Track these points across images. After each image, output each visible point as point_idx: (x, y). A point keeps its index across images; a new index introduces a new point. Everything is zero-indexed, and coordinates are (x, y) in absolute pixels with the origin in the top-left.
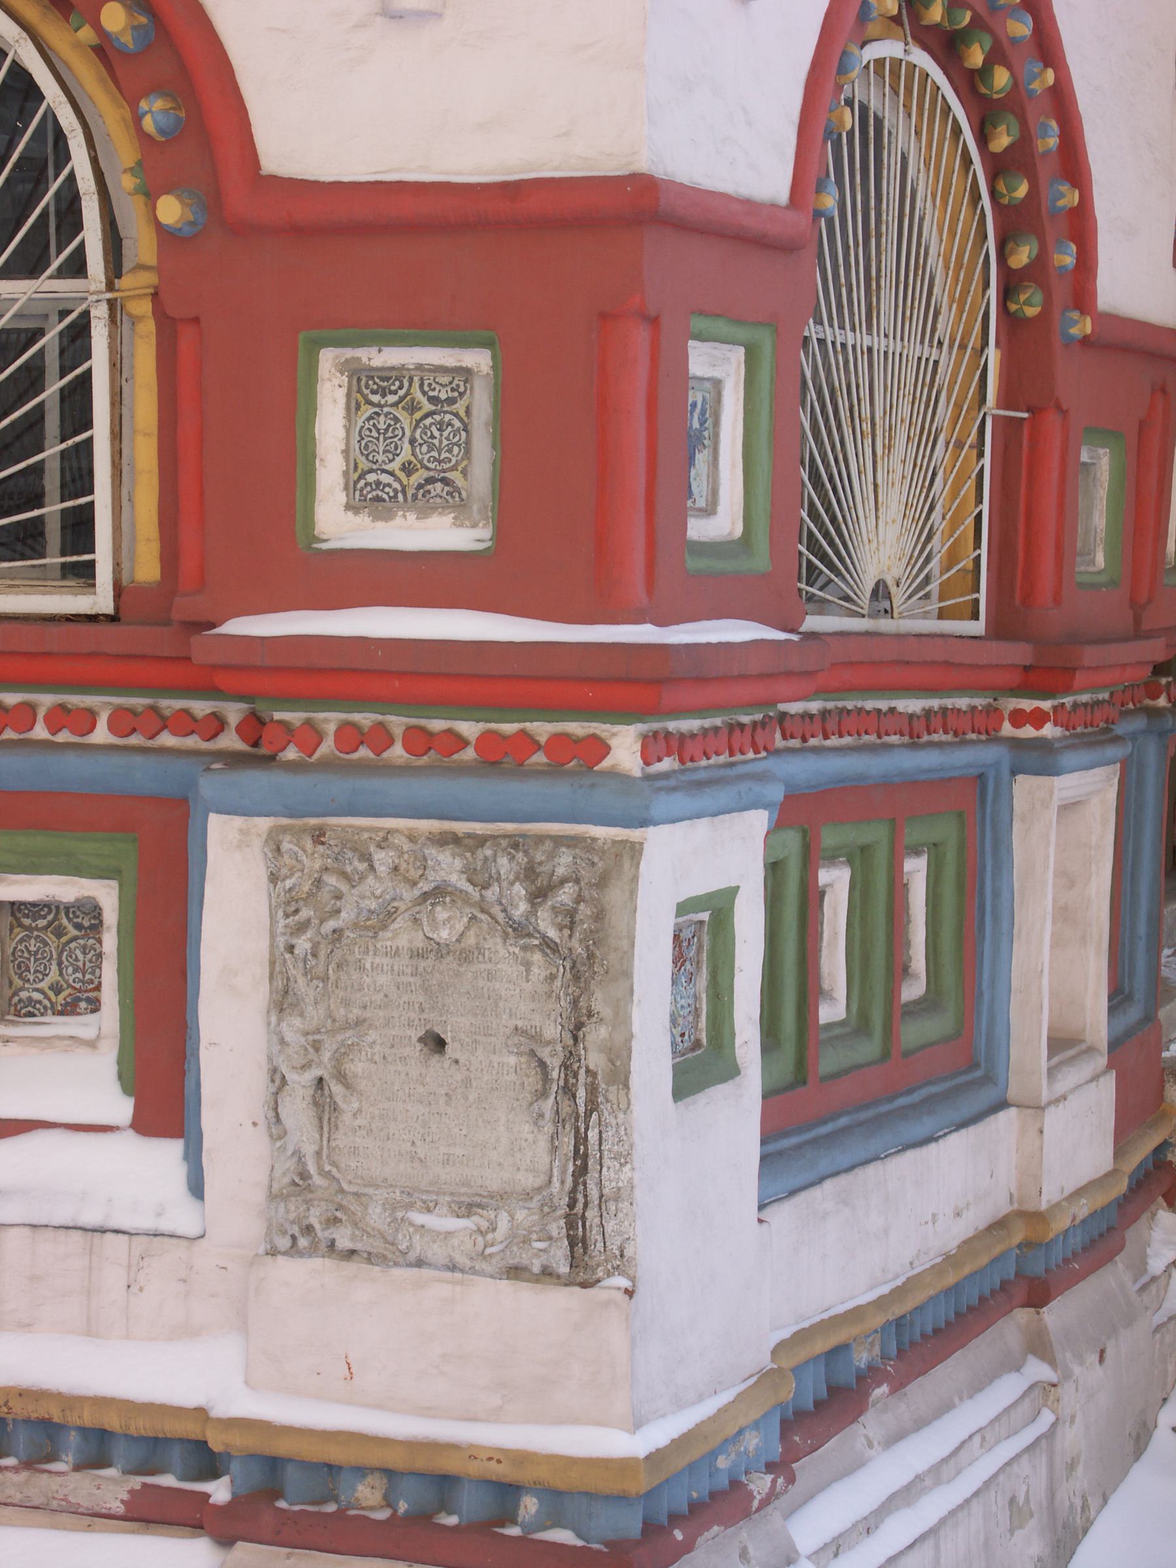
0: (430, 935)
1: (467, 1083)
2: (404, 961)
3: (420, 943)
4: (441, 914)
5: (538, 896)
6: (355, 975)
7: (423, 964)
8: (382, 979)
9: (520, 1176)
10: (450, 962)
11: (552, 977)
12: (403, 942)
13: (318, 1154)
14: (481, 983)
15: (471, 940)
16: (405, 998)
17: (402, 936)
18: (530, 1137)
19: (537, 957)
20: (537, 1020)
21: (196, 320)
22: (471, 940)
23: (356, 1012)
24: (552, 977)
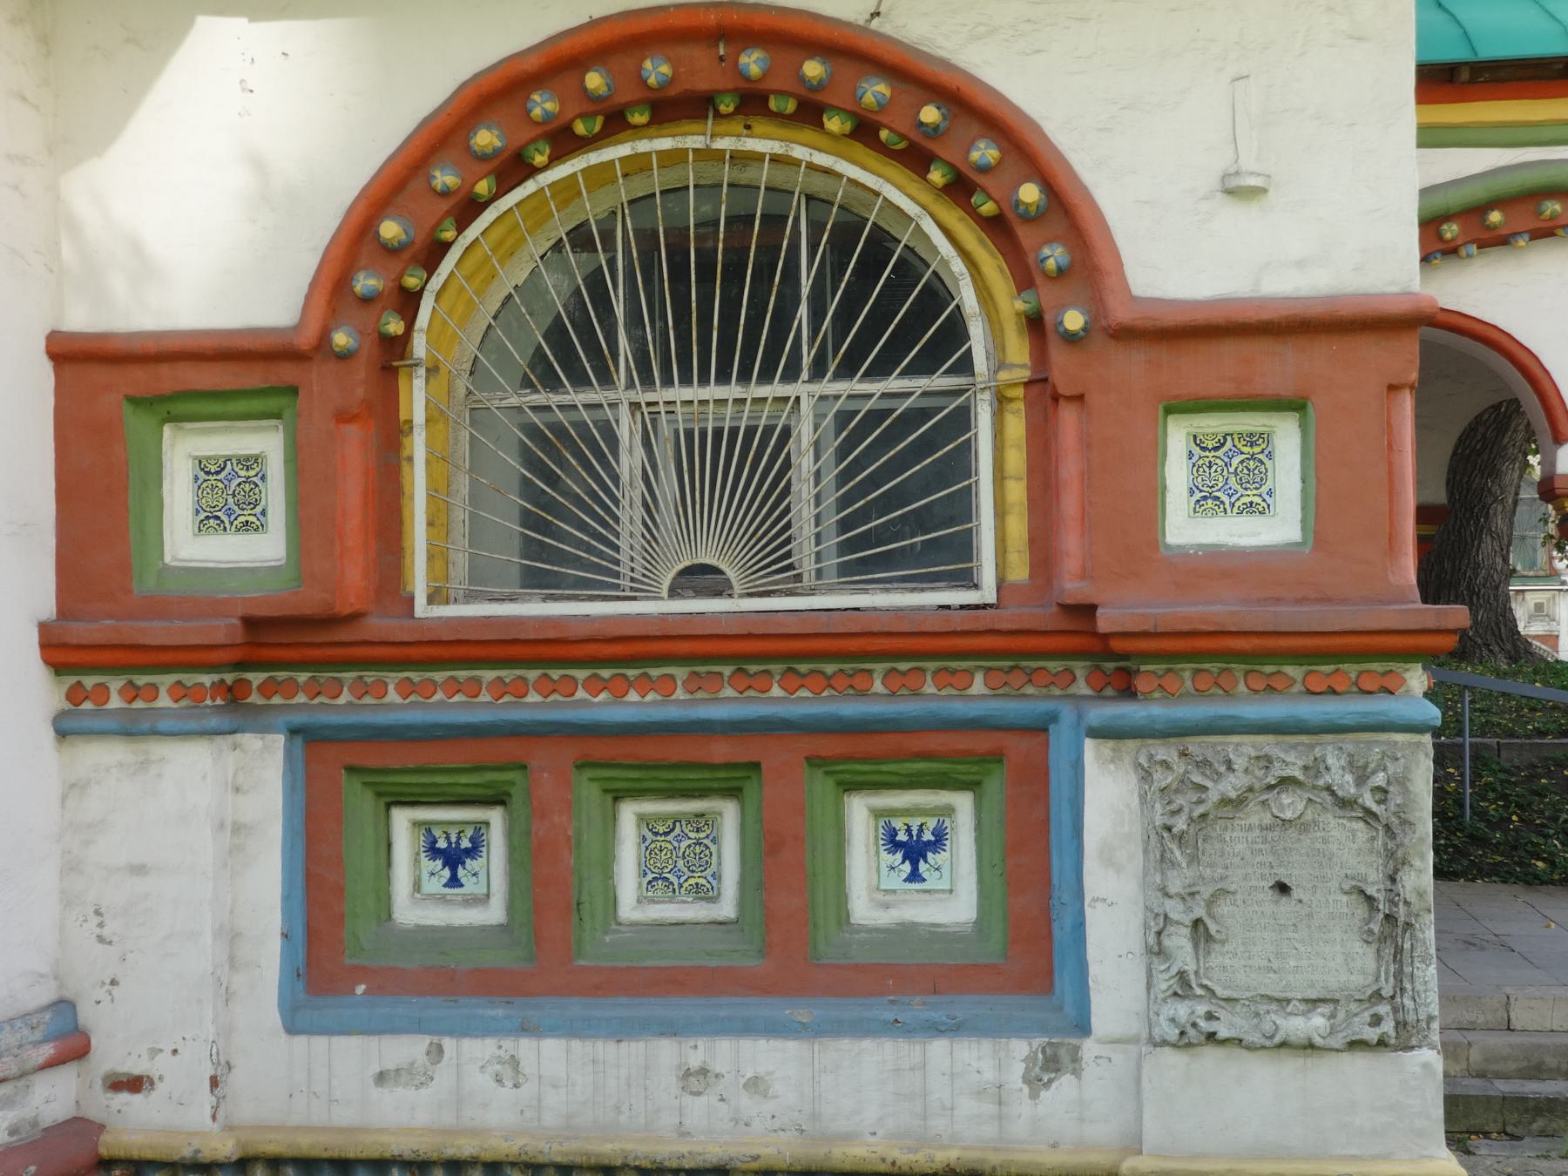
0: (1275, 811)
1: (1310, 916)
2: (1257, 832)
3: (1267, 819)
4: (1286, 799)
5: (1361, 780)
6: (1218, 846)
7: (1270, 835)
8: (1240, 847)
9: (1353, 978)
10: (1292, 833)
11: (1373, 839)
12: (1254, 820)
13: (1196, 973)
14: (1318, 846)
15: (1309, 816)
16: (1258, 859)
17: (1255, 816)
18: (1361, 951)
19: (1361, 825)
20: (1363, 870)
21: (1080, 398)
22: (1309, 816)
23: (1220, 871)
24: (1373, 839)
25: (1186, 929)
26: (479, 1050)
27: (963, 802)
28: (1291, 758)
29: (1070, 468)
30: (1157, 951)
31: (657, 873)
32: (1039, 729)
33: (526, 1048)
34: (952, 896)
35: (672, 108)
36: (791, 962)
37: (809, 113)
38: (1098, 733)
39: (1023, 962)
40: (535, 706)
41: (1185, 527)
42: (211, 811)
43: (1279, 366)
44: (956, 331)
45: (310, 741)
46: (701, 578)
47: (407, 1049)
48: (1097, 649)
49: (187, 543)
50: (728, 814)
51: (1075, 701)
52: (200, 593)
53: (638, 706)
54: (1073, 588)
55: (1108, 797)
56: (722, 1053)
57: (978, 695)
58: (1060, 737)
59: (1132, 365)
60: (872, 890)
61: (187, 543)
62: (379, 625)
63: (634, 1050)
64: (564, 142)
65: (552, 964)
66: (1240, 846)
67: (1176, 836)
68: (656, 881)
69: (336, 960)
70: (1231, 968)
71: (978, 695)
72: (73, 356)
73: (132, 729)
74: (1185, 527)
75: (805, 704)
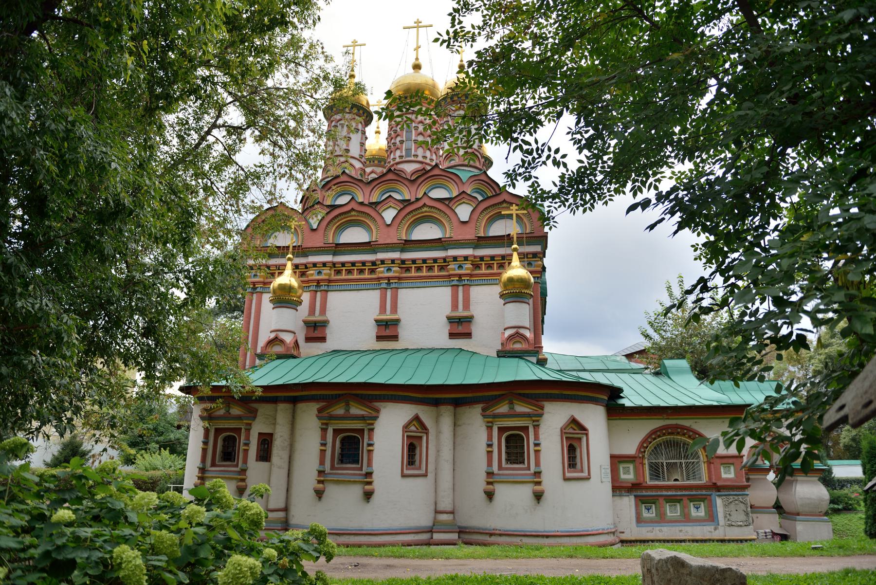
25: (727, 515)
26: (658, 528)
27: (702, 504)
28: (736, 498)
29: (713, 470)
30: (725, 517)
31: (672, 512)
32: (710, 495)
33: (662, 528)
34: (702, 513)
35: (669, 434)
36: (686, 519)
37: (684, 435)
38: (719, 496)
39: (712, 517)
40: (659, 493)
41: (724, 476)
42: (628, 503)
43: (731, 461)
44: (699, 457)
45: (635, 496)
46: (676, 480)
47: (650, 528)
48: (716, 488)
49: (623, 476)
50: (678, 505)
51: (714, 493)
52: (626, 481)
53: (670, 493)
54: (714, 481)
55: (719, 502)
56: (683, 528)
57: (704, 492)
58: (713, 497)
59: (718, 460)
60: (694, 513)
61: (623, 476)
62: (644, 484)
63: (674, 528)
64: (659, 436)
65: (662, 519)
66: (732, 506)
67: (725, 506)
68: (671, 512)
69: (639, 520)
70: (733, 518)
71: (704, 492)
72: (612, 457)
73: (620, 496)
74: (724, 476)
75: (687, 493)
